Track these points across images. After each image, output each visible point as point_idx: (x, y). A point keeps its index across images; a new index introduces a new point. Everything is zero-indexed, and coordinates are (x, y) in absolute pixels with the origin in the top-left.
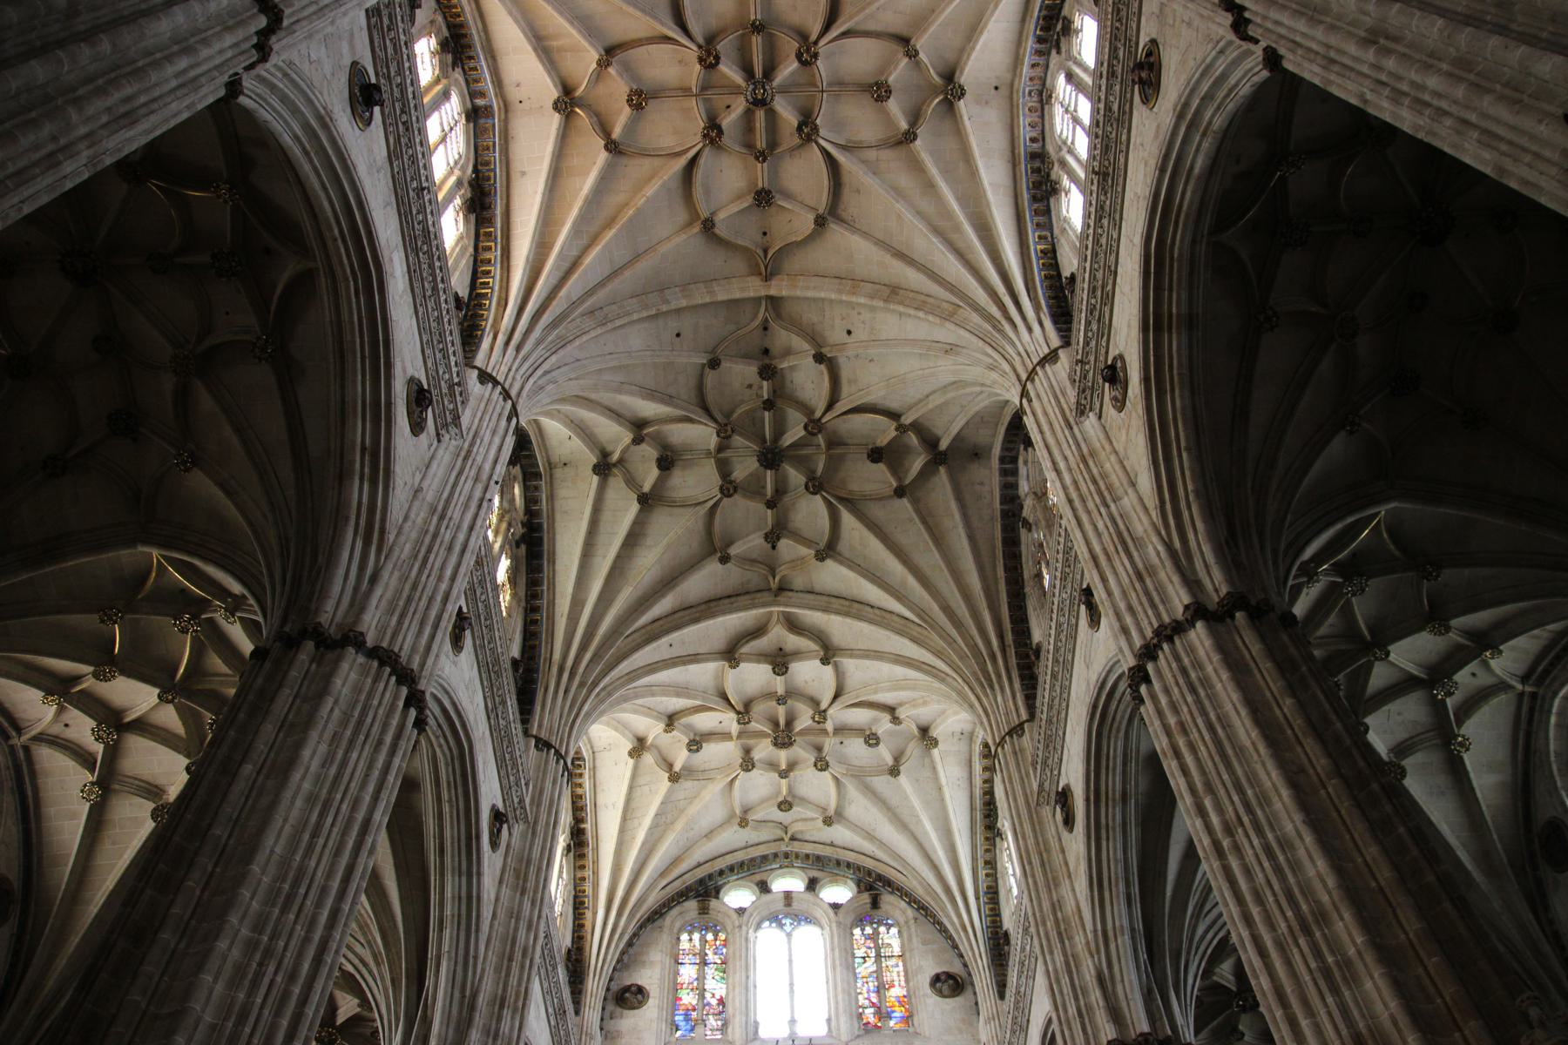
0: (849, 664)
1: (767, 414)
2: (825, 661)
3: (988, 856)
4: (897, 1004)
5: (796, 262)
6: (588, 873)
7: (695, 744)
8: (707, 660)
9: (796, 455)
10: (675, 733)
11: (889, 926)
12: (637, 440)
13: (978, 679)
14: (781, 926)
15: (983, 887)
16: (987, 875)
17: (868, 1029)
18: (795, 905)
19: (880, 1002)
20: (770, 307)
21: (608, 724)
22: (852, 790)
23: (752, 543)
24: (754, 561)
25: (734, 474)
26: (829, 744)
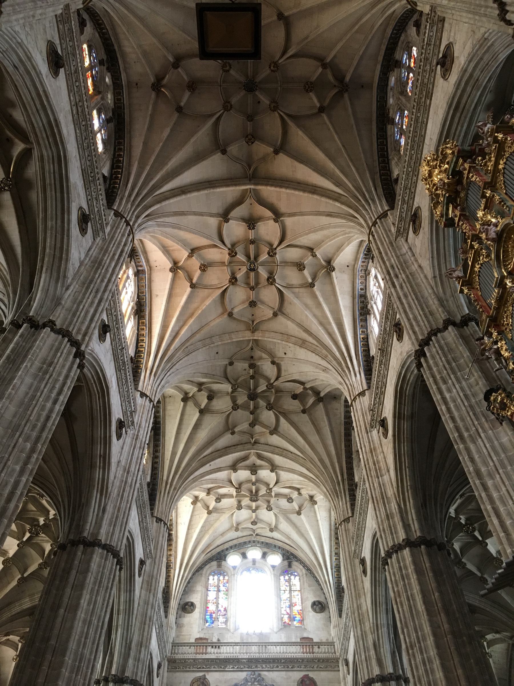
1: (251, 380)
2: (272, 471)
3: (337, 551)
4: (297, 614)
5: (264, 327)
6: (173, 553)
7: (218, 500)
10: (211, 496)
11: (295, 576)
12: (200, 390)
14: (250, 572)
15: (334, 564)
16: (336, 559)
18: (257, 564)
19: (290, 612)
20: (254, 342)
22: (281, 519)
23: (244, 426)
24: (245, 432)
26: (273, 500)
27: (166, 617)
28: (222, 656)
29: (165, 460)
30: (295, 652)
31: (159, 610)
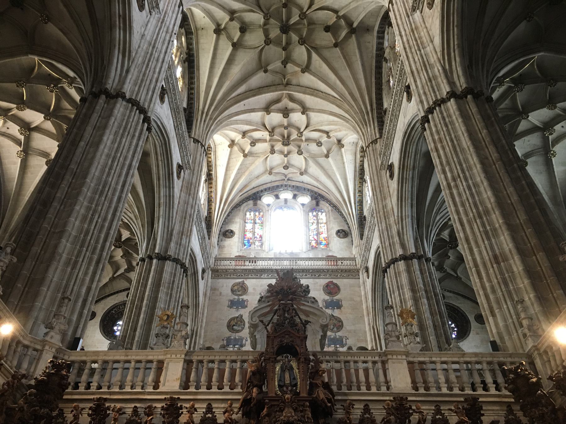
0: (312, 115)
1: (284, 9)
2: (303, 113)
3: (360, 189)
6: (213, 190)
8: (258, 111)
9: (295, 28)
11: (322, 212)
12: (232, 19)
13: (361, 122)
14: (283, 210)
15: (357, 200)
16: (359, 196)
21: (221, 135)
22: (311, 163)
23: (276, 65)
24: (277, 72)
25: (270, 36)
26: (303, 145)
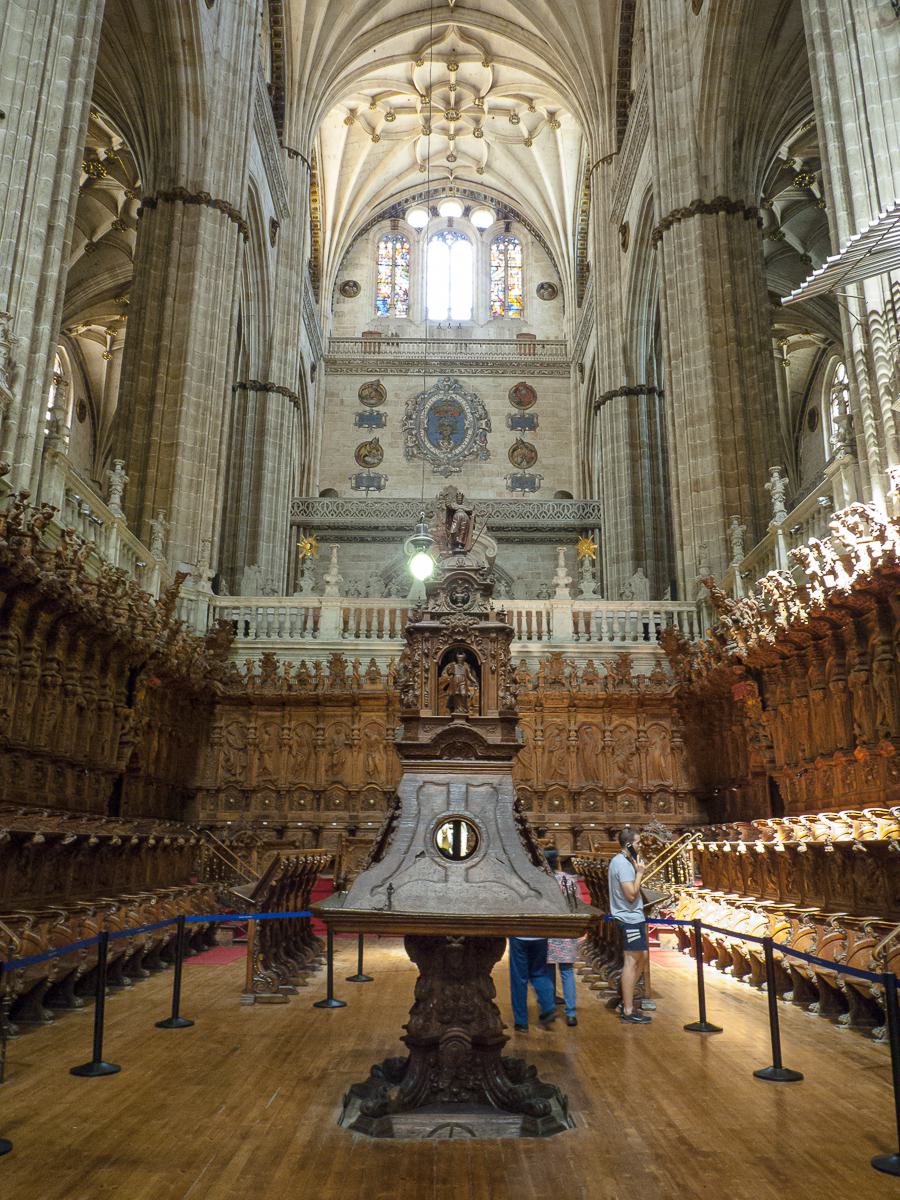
2: (486, 64)
3: (585, 207)
6: (318, 205)
14: (444, 240)
15: (578, 229)
17: (496, 317)
22: (498, 150)
26: (486, 119)
27: (317, 302)
28: (404, 357)
29: (294, 41)
30: (509, 353)
31: (307, 293)
